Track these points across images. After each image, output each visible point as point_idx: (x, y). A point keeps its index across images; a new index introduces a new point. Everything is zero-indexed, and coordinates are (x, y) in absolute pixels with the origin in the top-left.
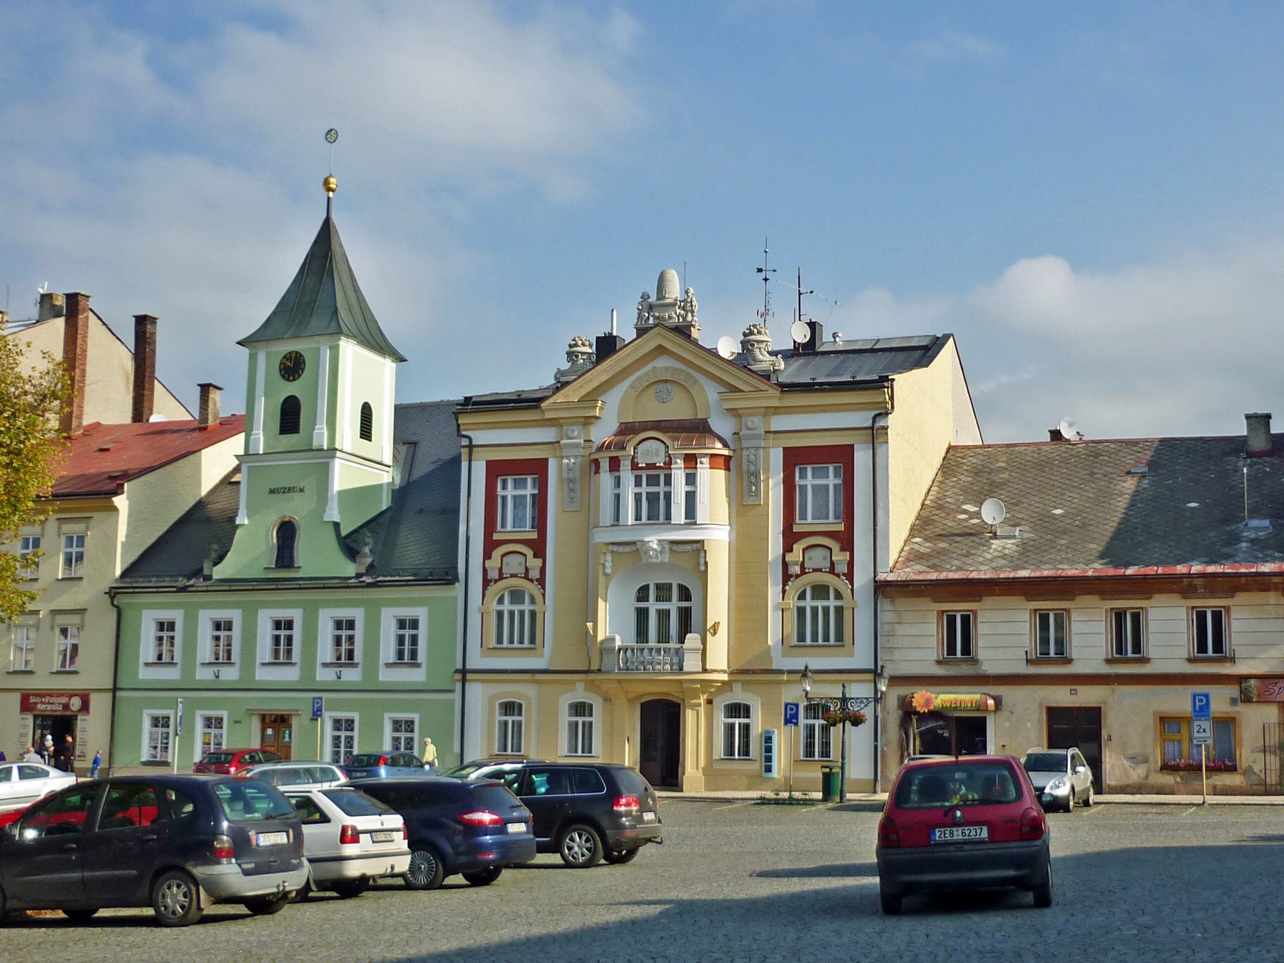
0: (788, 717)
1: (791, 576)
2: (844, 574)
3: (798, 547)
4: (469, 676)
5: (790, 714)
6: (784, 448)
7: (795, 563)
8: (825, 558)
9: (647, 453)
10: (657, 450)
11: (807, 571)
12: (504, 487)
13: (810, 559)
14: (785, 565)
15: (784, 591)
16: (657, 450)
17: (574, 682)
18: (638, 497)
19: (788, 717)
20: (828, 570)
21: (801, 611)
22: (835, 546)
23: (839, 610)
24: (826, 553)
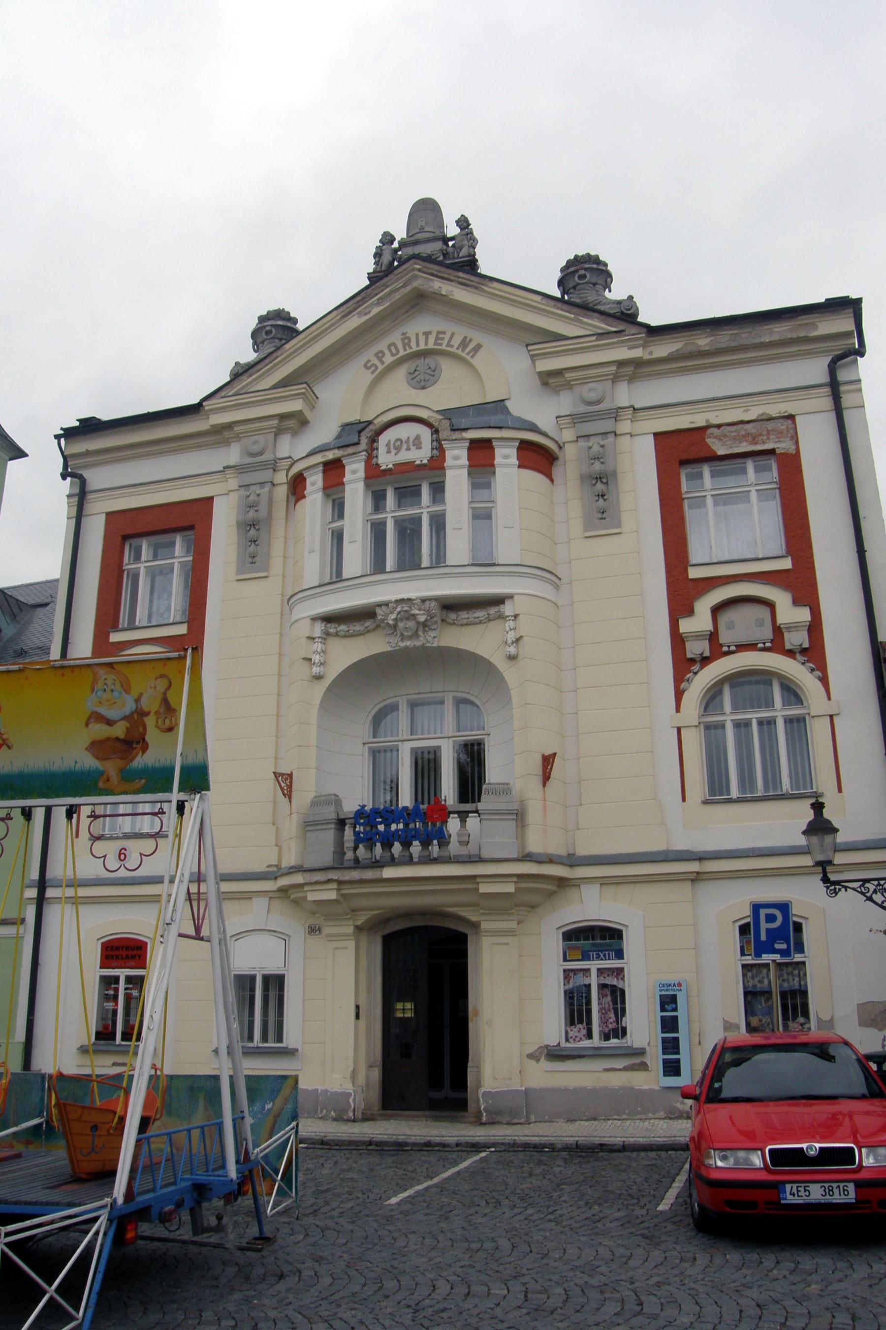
0: (763, 937)
1: (692, 661)
2: (804, 651)
3: (704, 606)
4: (50, 893)
5: (768, 931)
6: (656, 435)
7: (698, 636)
8: (760, 623)
9: (398, 445)
10: (418, 438)
11: (725, 649)
12: (137, 558)
13: (731, 626)
14: (678, 640)
15: (679, 695)
16: (418, 438)
17: (247, 896)
18: (378, 532)
19: (763, 937)
20: (768, 645)
21: (712, 730)
22: (781, 598)
23: (796, 725)
24: (763, 613)
